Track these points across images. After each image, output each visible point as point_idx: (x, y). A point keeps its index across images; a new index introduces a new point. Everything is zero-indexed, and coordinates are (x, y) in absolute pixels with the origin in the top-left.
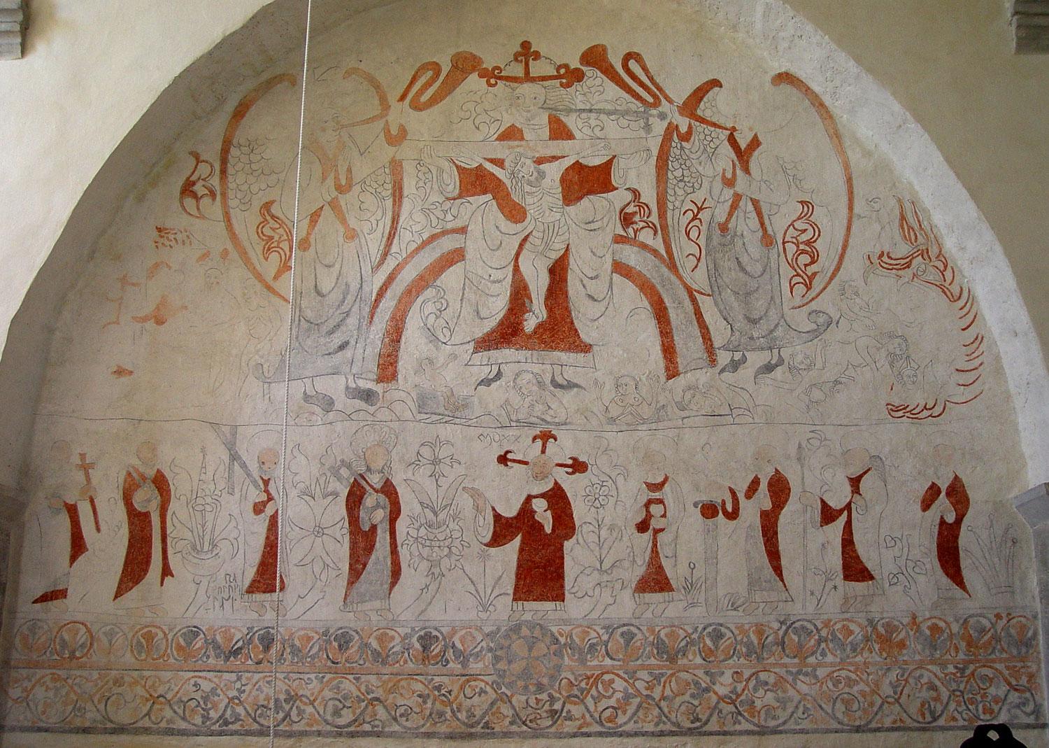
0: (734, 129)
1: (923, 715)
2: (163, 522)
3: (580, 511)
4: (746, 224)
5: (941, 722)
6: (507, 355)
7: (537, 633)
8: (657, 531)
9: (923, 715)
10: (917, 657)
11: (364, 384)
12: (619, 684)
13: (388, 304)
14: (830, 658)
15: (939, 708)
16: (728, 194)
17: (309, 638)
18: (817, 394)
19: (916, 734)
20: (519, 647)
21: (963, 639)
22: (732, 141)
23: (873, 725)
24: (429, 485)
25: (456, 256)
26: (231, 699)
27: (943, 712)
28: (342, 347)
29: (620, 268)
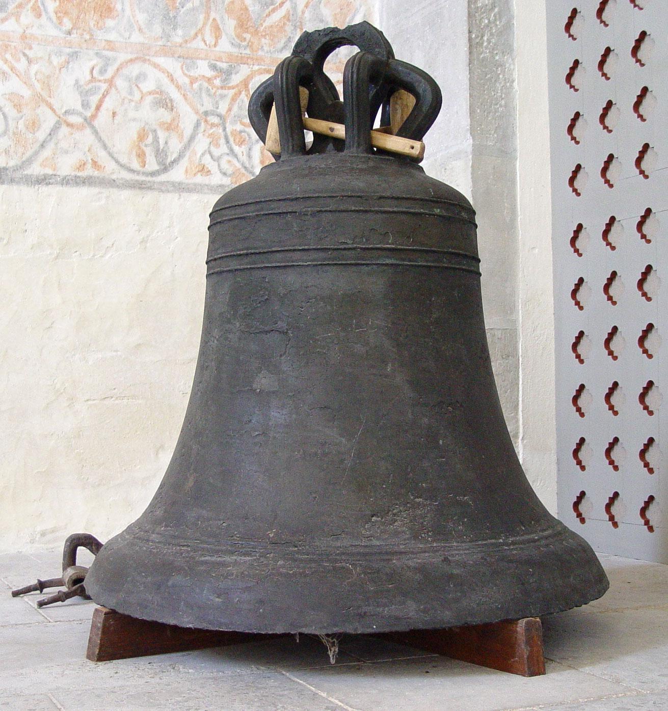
1: (141, 155)
5: (177, 175)
9: (141, 155)
10: (136, 38)
15: (175, 146)
19: (126, 194)
21: (229, 11)
23: (36, 169)
27: (180, 156)
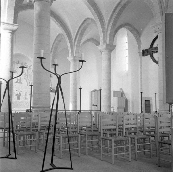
3: (21, 94)
6: (17, 83)
29: (24, 78)
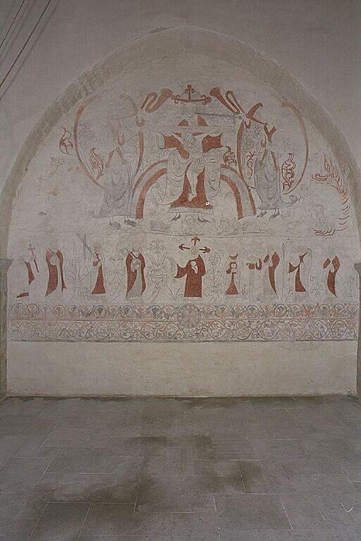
0: (266, 124)
2: (61, 269)
4: (269, 162)
5: (323, 338)
7: (193, 308)
8: (233, 273)
11: (131, 219)
12: (219, 325)
13: (138, 192)
14: (289, 317)
16: (263, 150)
17: (115, 310)
18: (291, 226)
20: (187, 312)
22: (266, 129)
24: (155, 256)
25: (163, 172)
26: (88, 330)
28: (123, 205)
29: (222, 177)
